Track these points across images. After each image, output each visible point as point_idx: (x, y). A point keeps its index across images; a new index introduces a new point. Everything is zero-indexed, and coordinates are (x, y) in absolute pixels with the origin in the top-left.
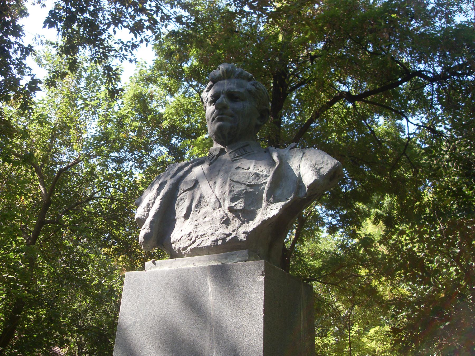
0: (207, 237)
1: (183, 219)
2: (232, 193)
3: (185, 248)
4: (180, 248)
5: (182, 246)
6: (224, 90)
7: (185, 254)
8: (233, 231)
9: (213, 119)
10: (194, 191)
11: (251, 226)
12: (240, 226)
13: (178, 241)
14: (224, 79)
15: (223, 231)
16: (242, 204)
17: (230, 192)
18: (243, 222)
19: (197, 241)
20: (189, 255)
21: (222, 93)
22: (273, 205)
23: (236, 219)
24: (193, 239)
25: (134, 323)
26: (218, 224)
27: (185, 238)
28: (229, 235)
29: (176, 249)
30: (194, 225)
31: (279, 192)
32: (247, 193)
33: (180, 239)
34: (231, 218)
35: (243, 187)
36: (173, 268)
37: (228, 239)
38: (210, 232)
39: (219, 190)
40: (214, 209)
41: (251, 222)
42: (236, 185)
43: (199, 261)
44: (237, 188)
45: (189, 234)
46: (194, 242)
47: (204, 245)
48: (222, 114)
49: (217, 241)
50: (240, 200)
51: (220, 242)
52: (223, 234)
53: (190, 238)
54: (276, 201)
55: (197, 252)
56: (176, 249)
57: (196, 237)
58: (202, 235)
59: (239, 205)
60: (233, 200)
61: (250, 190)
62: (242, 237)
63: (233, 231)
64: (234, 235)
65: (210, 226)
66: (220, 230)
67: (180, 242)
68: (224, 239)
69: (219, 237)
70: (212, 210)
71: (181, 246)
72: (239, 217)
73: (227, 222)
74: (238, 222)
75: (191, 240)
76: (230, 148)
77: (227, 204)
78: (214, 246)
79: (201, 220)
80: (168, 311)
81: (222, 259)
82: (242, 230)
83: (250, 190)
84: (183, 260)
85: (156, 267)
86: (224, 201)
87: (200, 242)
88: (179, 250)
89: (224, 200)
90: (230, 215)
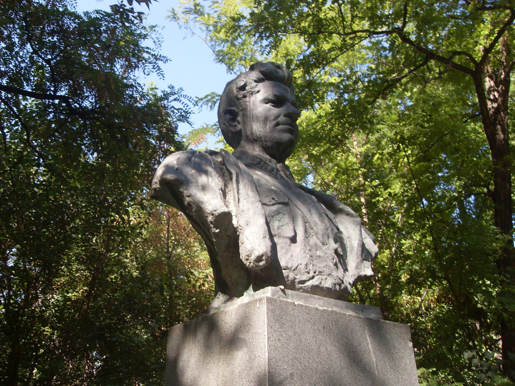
1: (288, 241)
3: (303, 282)
4: (295, 279)
5: (299, 278)
7: (301, 288)
9: (278, 124)
13: (294, 270)
14: (285, 84)
19: (316, 278)
20: (305, 291)
22: (365, 262)
24: (311, 274)
25: (292, 375)
26: (331, 265)
27: (302, 267)
29: (290, 279)
30: (308, 256)
38: (327, 271)
43: (336, 306)
46: (313, 277)
49: (335, 284)
56: (290, 279)
58: (320, 272)
67: (296, 272)
70: (321, 245)
71: (296, 277)
75: (309, 273)
78: (334, 289)
80: (332, 365)
84: (319, 299)
85: (287, 298)
86: (328, 238)
88: (293, 282)
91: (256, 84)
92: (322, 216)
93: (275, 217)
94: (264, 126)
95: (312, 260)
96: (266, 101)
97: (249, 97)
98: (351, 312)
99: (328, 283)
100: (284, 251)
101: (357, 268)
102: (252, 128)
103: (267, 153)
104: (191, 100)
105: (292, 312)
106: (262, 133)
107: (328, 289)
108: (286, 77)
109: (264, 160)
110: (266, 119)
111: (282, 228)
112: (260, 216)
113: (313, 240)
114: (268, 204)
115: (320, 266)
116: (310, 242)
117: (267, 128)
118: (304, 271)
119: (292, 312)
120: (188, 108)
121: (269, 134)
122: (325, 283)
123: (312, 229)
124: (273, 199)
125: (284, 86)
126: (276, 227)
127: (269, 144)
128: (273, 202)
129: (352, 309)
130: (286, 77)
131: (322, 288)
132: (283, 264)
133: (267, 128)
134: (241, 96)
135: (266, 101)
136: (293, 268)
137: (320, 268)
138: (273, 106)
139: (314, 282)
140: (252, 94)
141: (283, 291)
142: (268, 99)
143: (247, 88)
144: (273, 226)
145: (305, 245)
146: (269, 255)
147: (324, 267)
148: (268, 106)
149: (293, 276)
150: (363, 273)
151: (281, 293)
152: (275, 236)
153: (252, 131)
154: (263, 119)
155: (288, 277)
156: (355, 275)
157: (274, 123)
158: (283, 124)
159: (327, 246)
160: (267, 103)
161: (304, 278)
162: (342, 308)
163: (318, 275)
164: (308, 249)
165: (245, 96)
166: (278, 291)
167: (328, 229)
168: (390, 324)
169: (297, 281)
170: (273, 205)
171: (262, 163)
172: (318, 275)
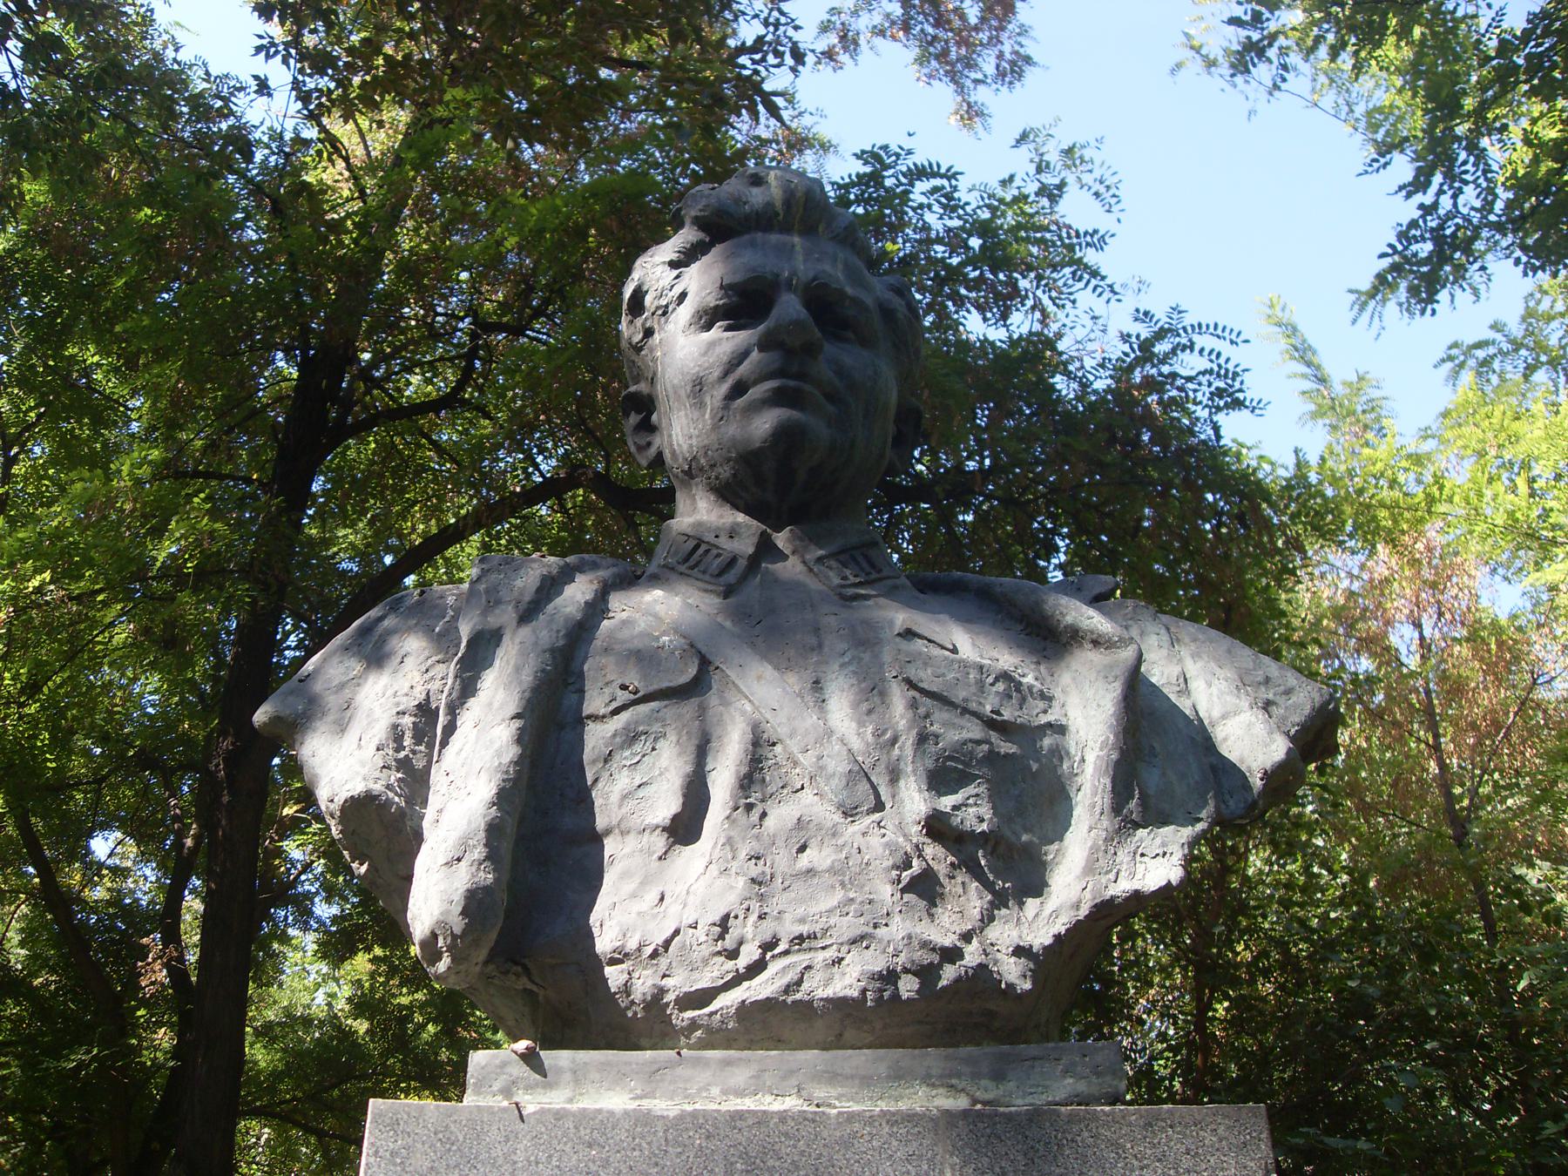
0: (831, 953)
1: (660, 842)
2: (931, 748)
3: (702, 998)
4: (662, 991)
5: (679, 983)
6: (793, 273)
7: (694, 1025)
8: (967, 937)
9: (739, 389)
10: (702, 711)
12: (988, 918)
14: (786, 229)
16: (986, 811)
17: (922, 739)
18: (1000, 900)
19: (773, 968)
20: (717, 1037)
21: (789, 286)
22: (1141, 833)
23: (961, 876)
24: (749, 954)
26: (885, 892)
28: (951, 955)
29: (637, 995)
30: (741, 882)
31: (1152, 778)
32: (993, 757)
33: (667, 944)
34: (941, 869)
35: (974, 731)
36: (663, 1106)
37: (949, 973)
38: (847, 926)
39: (861, 724)
40: (849, 813)
41: (1032, 904)
42: (941, 715)
43: (833, 1077)
44: (956, 732)
45: (724, 924)
46: (756, 968)
47: (821, 993)
48: (801, 376)
49: (889, 977)
50: (971, 790)
51: (908, 987)
52: (925, 945)
53: (729, 942)
54: (1155, 817)
56: (637, 995)
57: (768, 946)
58: (800, 939)
61: (1007, 748)
62: (1012, 971)
63: (967, 937)
64: (972, 955)
65: (839, 895)
66: (898, 928)
67: (663, 962)
68: (926, 974)
69: (902, 959)
70: (837, 817)
71: (668, 982)
72: (976, 873)
74: (975, 900)
75: (733, 954)
77: (914, 801)
78: (879, 1000)
79: (781, 860)
81: (976, 1076)
82: (1004, 934)
83: (1007, 748)
84: (728, 1063)
85: (550, 1086)
87: (791, 976)
88: (656, 1001)
89: (894, 776)
90: (937, 856)
91: (676, 272)
92: (883, 694)
93: (617, 757)
94: (696, 414)
95: (762, 898)
96: (707, 319)
97: (661, 329)
98: (922, 1091)
99: (847, 982)
100: (629, 887)
101: (1090, 869)
102: (670, 436)
103: (738, 509)
104: (1219, 332)
105: (498, 1152)
106: (694, 442)
107: (839, 1004)
108: (778, 204)
109: (710, 538)
110: (698, 386)
111: (641, 793)
112: (484, 776)
114: (602, 711)
116: (770, 822)
117: (707, 416)
118: (706, 950)
119: (498, 1152)
120: (1222, 361)
121: (714, 437)
122: (828, 982)
123: (796, 764)
124: (624, 687)
125: (774, 238)
126: (615, 797)
127: (725, 472)
128: (623, 697)
129: (927, 1080)
130: (778, 204)
131: (806, 1007)
132: (604, 944)
133: (707, 416)
134: (641, 336)
135: (707, 319)
136: (648, 951)
137: (802, 921)
138: (728, 329)
139: (760, 988)
140: (664, 314)
141: (529, 1058)
142: (706, 312)
143: (648, 299)
144: (607, 796)
145: (729, 841)
146: (458, 930)
147: (830, 911)
148: (716, 332)
149: (650, 982)
150: (1123, 887)
151: (522, 1070)
152: (608, 832)
153: (671, 445)
154: (689, 388)
155: (627, 989)
156: (1077, 906)
157: (725, 388)
158: (756, 382)
159: (877, 816)
160: (708, 327)
161: (704, 981)
162: (866, 1081)
163: (786, 953)
164: (743, 855)
165: (649, 333)
166: (504, 1064)
167: (894, 741)
168: (1114, 1120)
169: (670, 997)
170: (616, 712)
171: (703, 548)
172: (786, 953)
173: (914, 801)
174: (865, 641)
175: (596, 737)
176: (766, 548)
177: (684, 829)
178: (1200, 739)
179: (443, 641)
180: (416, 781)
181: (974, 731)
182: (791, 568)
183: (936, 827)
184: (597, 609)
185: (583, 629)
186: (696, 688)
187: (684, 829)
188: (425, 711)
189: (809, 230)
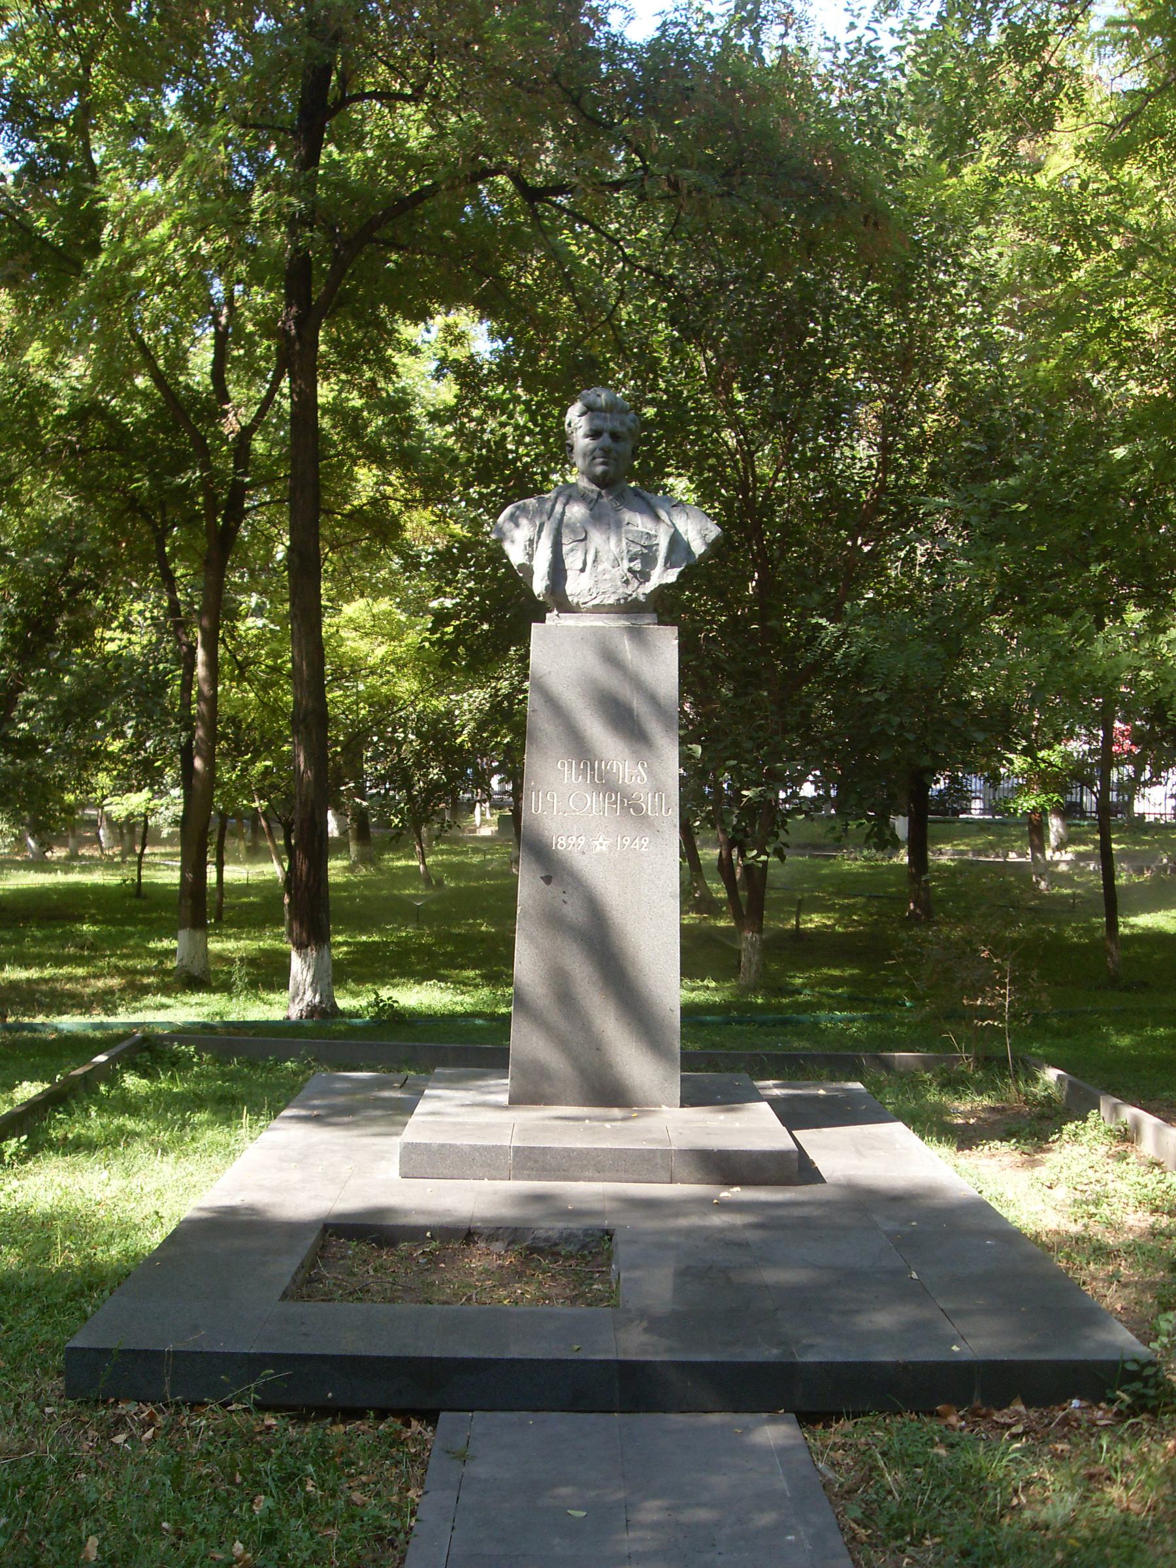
11: (649, 587)
15: (623, 590)
31: (674, 558)
35: (638, 548)
36: (581, 624)
44: (636, 549)
54: (672, 567)
55: (598, 609)
59: (637, 565)
60: (631, 560)
62: (642, 598)
73: (627, 582)
74: (636, 583)
76: (609, 494)
77: (626, 564)
90: (630, 575)
96: (586, 436)
99: (611, 601)
113: (601, 568)
115: (603, 587)
135: (586, 436)
173: (626, 564)
174: (619, 525)
175: (565, 549)
176: (600, 495)
177: (583, 570)
178: (688, 546)
179: (532, 521)
180: (531, 556)
181: (638, 548)
182: (605, 500)
183: (630, 570)
184: (563, 513)
185: (561, 521)
186: (585, 539)
187: (583, 570)
188: (531, 541)
189: (611, 411)
